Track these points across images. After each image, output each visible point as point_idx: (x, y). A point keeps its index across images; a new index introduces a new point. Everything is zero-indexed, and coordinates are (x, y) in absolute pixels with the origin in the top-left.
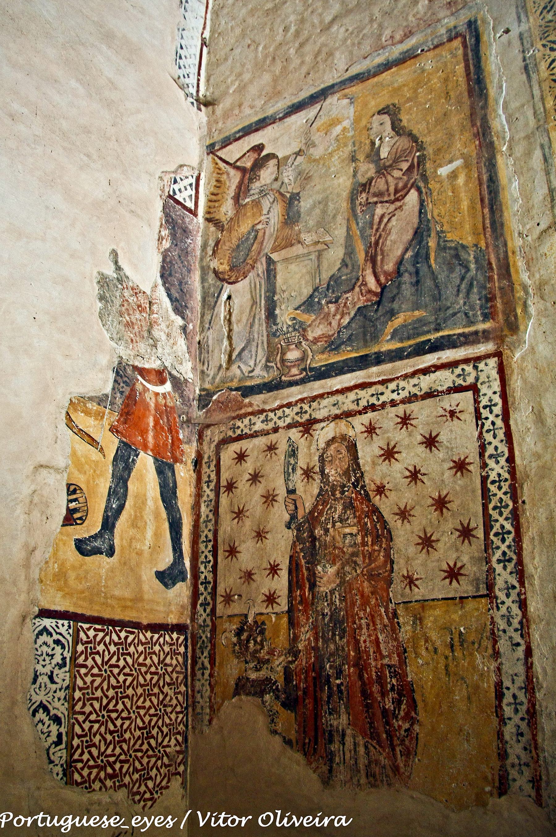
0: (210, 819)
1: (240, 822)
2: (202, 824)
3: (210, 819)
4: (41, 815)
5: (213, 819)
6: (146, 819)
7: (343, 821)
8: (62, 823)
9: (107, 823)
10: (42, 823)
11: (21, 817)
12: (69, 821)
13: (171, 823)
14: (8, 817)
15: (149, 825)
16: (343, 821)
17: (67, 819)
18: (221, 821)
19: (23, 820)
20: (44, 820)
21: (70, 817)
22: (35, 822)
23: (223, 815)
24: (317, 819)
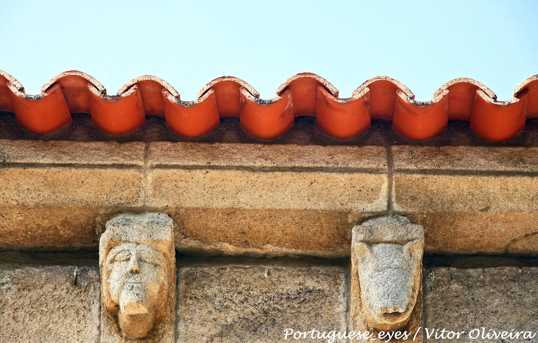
0: (434, 333)
1: (302, 335)
2: (428, 337)
3: (434, 333)
4: (313, 331)
5: (437, 333)
6: (388, 333)
7: (530, 335)
8: (328, 336)
9: (360, 336)
10: (314, 336)
11: (299, 332)
12: (334, 335)
13: (407, 336)
14: (290, 331)
15: (390, 337)
16: (530, 335)
17: (332, 333)
18: (442, 335)
19: (301, 334)
20: (315, 333)
21: (334, 332)
22: (309, 335)
23: (444, 331)
24: (511, 334)
